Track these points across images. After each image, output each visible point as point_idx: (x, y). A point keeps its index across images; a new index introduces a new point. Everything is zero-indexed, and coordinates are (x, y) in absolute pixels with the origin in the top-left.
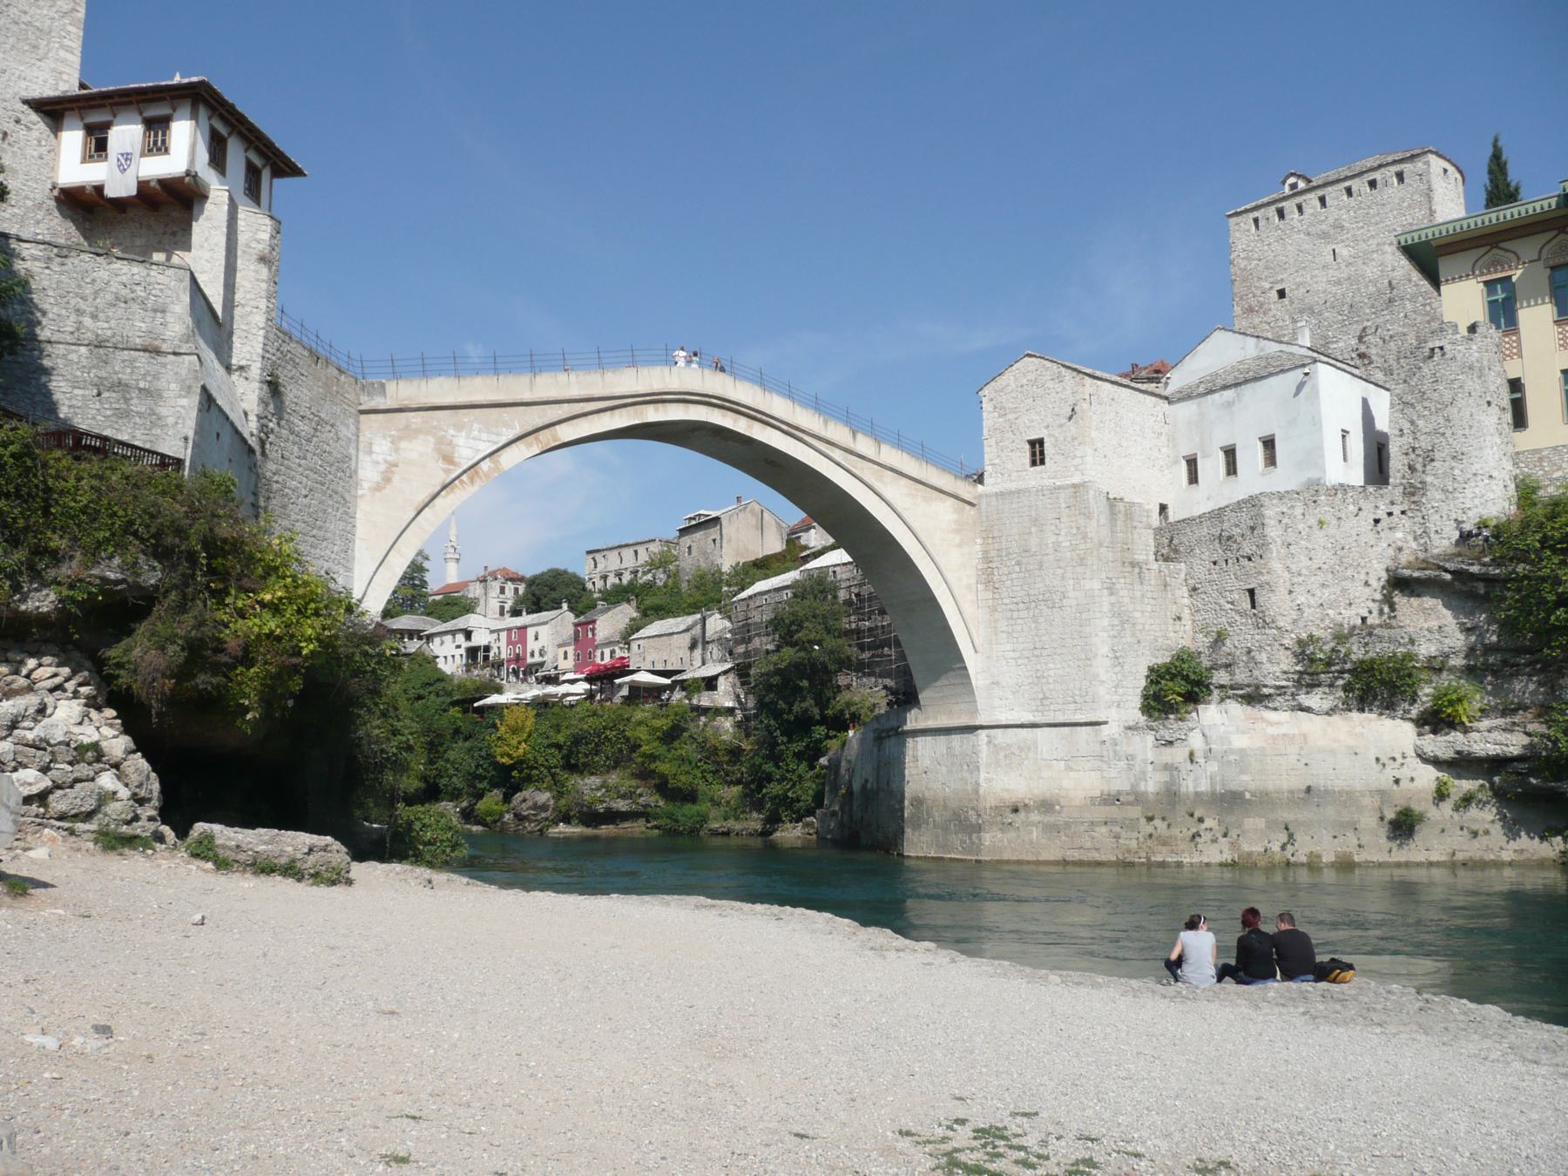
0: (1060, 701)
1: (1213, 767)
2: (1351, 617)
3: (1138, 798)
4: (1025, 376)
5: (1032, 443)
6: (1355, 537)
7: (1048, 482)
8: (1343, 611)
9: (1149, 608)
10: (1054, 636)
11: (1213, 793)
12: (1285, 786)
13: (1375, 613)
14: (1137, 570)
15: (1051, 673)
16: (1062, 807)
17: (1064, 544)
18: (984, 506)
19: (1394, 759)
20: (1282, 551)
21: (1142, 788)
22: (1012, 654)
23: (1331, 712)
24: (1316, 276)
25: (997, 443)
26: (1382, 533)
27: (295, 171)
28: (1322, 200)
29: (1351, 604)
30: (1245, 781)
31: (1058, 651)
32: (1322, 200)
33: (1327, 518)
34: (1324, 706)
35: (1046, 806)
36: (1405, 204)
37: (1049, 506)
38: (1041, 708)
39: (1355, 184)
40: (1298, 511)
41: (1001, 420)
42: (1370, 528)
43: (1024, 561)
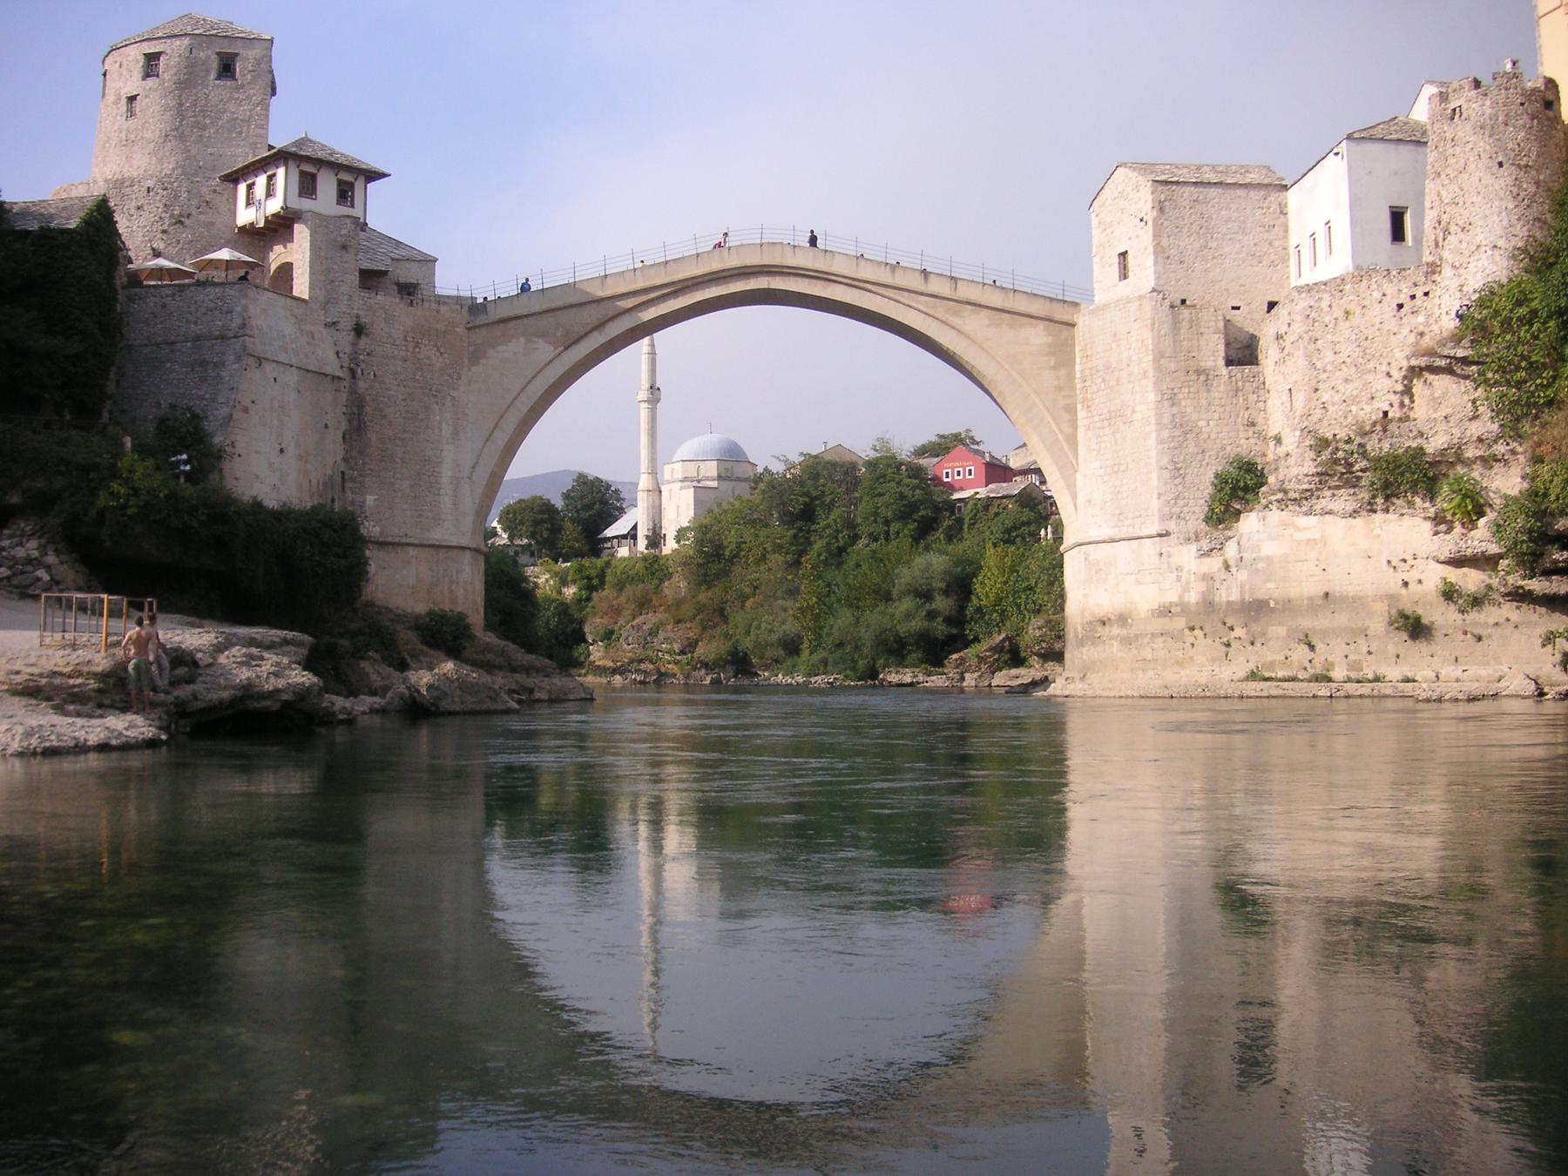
1: (1242, 576)
2: (1368, 413)
3: (1184, 608)
4: (1117, 188)
5: (1120, 254)
6: (1378, 326)
8: (1365, 407)
9: (1216, 416)
11: (1243, 601)
12: (1305, 592)
13: (1396, 405)
14: (1203, 378)
16: (1133, 620)
17: (1135, 358)
19: (1404, 561)
20: (1310, 347)
21: (1186, 599)
23: (1354, 514)
26: (1404, 319)
27: (384, 175)
29: (1373, 398)
30: (1269, 589)
33: (1352, 307)
34: (1347, 508)
35: (1123, 619)
40: (1325, 304)
42: (1392, 314)
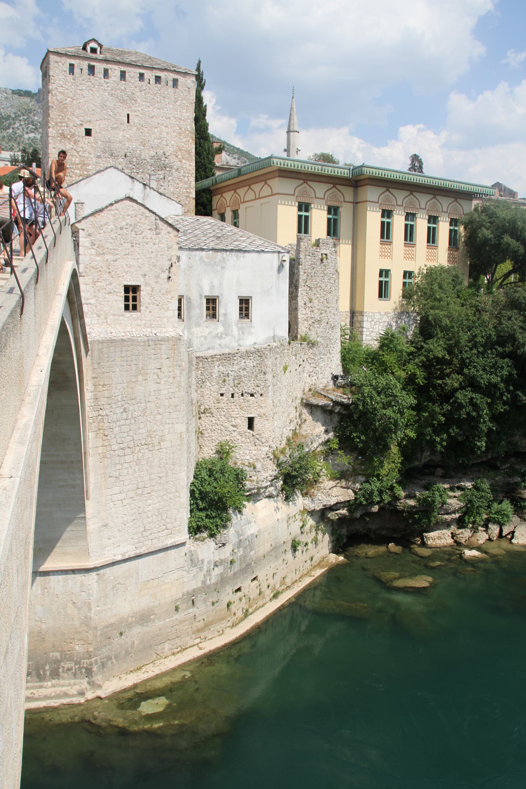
0: (155, 530)
5: (127, 289)
7: (148, 331)
10: (153, 476)
15: (150, 508)
17: (164, 392)
18: (96, 353)
21: (208, 582)
22: (120, 497)
24: (114, 128)
25: (94, 282)
28: (123, 75)
31: (156, 488)
32: (123, 75)
37: (153, 356)
38: (142, 539)
39: (149, 75)
41: (98, 258)
43: (131, 408)
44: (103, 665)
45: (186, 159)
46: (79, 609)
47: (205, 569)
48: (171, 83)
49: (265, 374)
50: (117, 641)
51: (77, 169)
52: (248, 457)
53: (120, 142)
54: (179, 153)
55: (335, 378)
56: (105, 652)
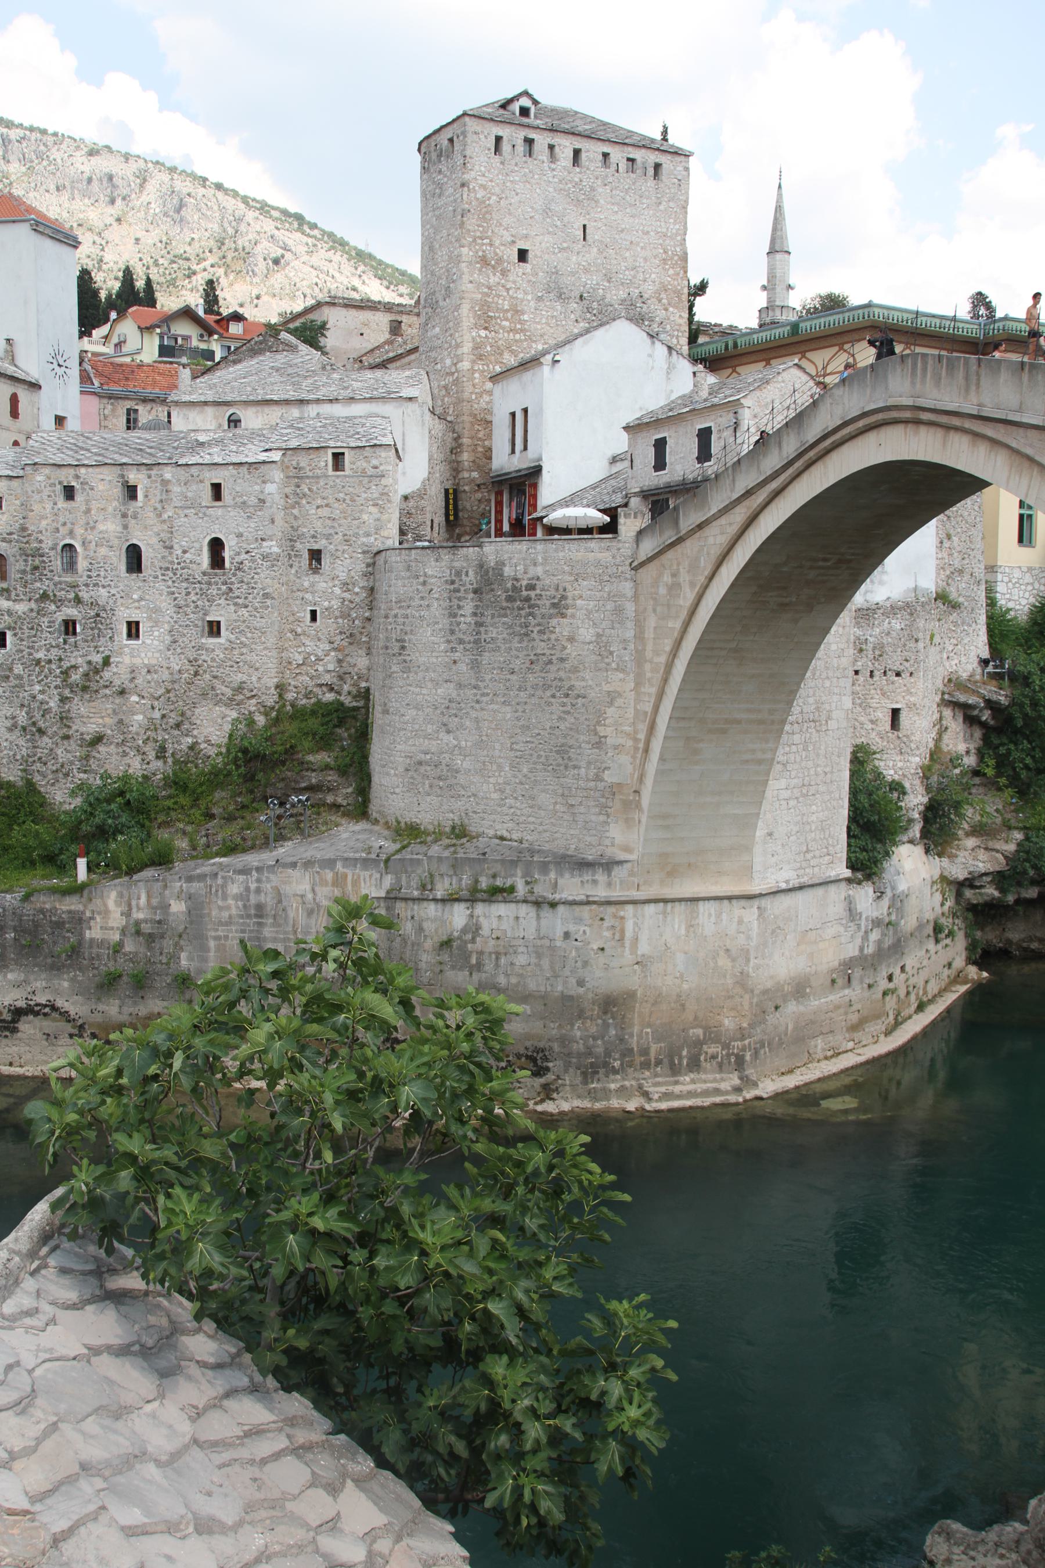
0: (817, 853)
15: (814, 818)
36: (662, 207)
38: (804, 864)
39: (617, 155)
44: (756, 1053)
45: (674, 307)
46: (733, 960)
47: (863, 929)
48: (651, 171)
49: (917, 641)
50: (772, 1019)
51: (506, 319)
52: (892, 772)
53: (573, 274)
54: (663, 296)
55: (985, 662)
56: (758, 1034)
